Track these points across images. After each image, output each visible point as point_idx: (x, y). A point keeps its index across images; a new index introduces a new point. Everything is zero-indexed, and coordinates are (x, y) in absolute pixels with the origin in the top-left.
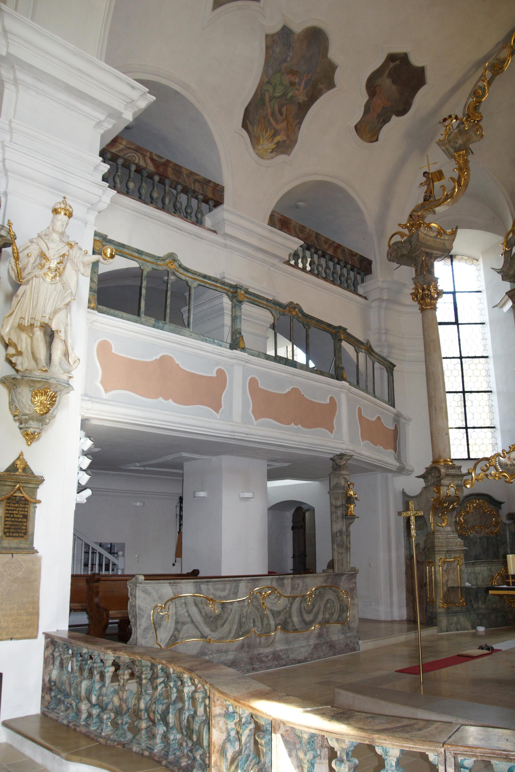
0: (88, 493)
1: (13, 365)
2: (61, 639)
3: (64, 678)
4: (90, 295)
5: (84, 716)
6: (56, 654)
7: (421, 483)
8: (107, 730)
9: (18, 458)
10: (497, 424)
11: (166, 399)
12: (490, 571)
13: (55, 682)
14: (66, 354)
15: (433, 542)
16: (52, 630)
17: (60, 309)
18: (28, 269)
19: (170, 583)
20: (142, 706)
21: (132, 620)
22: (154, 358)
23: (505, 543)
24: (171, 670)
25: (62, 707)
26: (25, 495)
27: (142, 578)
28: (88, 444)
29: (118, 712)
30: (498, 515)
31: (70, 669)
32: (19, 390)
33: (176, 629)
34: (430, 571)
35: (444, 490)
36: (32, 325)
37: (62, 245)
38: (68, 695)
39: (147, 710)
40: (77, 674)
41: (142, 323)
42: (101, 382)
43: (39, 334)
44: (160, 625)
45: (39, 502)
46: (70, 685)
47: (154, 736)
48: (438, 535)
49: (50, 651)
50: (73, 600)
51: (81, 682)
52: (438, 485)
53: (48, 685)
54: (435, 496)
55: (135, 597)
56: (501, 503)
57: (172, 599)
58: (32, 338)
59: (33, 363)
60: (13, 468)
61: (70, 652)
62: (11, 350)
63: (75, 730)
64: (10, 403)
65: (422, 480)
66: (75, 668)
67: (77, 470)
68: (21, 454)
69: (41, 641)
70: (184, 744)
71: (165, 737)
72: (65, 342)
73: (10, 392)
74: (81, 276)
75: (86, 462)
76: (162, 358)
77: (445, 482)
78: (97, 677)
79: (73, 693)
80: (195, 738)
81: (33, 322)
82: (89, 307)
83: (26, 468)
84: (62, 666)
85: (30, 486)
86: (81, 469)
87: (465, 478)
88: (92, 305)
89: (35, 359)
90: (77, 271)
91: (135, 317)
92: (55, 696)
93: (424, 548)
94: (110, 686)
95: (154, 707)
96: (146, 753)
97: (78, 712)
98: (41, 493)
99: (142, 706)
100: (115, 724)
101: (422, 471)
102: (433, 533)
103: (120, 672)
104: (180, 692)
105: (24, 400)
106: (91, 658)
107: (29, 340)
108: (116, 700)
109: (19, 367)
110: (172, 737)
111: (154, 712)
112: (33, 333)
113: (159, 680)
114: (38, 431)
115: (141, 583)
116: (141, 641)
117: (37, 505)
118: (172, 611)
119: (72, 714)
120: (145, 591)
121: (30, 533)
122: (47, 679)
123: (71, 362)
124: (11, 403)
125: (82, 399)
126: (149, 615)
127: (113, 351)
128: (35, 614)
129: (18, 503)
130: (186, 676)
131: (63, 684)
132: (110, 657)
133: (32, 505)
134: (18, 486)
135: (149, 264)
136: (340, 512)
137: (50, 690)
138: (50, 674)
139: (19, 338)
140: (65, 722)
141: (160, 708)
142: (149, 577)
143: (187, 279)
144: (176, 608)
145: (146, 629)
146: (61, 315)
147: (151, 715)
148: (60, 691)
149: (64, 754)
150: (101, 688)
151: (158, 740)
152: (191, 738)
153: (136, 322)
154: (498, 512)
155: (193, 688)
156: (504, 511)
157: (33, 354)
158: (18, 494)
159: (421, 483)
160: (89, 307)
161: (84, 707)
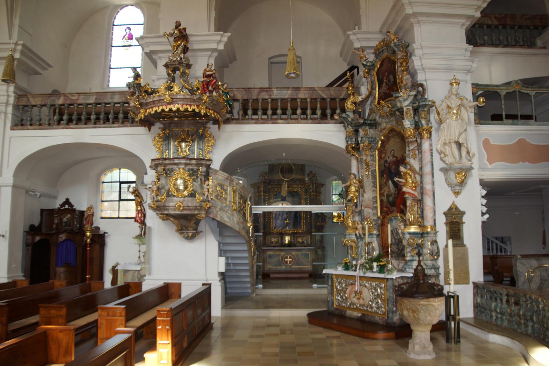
0: (487, 216)
1: (444, 162)
2: (481, 284)
3: (484, 302)
4: (475, 117)
5: (494, 318)
6: (479, 292)
8: (505, 323)
9: (453, 204)
11: (524, 162)
13: (479, 304)
14: (468, 153)
16: (476, 281)
17: (462, 133)
18: (444, 116)
19: (536, 259)
20: (521, 313)
21: (516, 278)
22: (514, 142)
24: (533, 297)
25: (484, 315)
26: (457, 220)
27: (519, 257)
28: (484, 192)
29: (511, 315)
31: (486, 298)
32: (449, 173)
33: (541, 283)
36: (450, 143)
37: (458, 100)
38: (486, 309)
39: (523, 315)
40: (490, 300)
41: (505, 124)
42: (487, 160)
43: (454, 146)
44: (531, 281)
45: (464, 223)
46: (487, 305)
47: (528, 326)
49: (475, 291)
50: (485, 268)
51: (492, 303)
53: (476, 305)
55: (517, 266)
57: (537, 268)
58: (451, 148)
59: (453, 159)
60: (451, 209)
61: (485, 290)
62: (442, 155)
63: (490, 323)
64: (445, 180)
66: (488, 297)
67: (480, 205)
68: (454, 202)
69: (471, 286)
70: (541, 329)
71: (533, 326)
72: (467, 148)
73: (445, 174)
74: (469, 113)
75: (484, 201)
76: (519, 140)
78: (499, 301)
79: (488, 308)
80: (545, 326)
81: (450, 141)
82: (475, 124)
83: (457, 208)
84: (482, 297)
85: (459, 216)
86: (482, 205)
88: (477, 122)
89: (454, 158)
90: (467, 110)
91: (500, 122)
92: (480, 310)
94: (505, 305)
95: (526, 313)
96: (524, 333)
97: (491, 316)
98: (465, 219)
99: (521, 313)
100: (510, 322)
103: (510, 298)
104: (538, 307)
105: (452, 178)
106: (496, 293)
107: (450, 149)
108: (509, 310)
109: (447, 162)
110: (536, 326)
111: (527, 316)
112: (451, 146)
113: (528, 302)
114: (460, 190)
115: (519, 259)
116: (521, 287)
117: (464, 224)
118: (538, 273)
119: (488, 317)
120: (522, 264)
121: (461, 237)
122: (475, 302)
123: (471, 156)
124: (446, 179)
125: (479, 171)
126: (525, 275)
127: (491, 143)
128: (467, 273)
129: (455, 224)
130: (540, 300)
131: (483, 304)
132: (504, 292)
133: (461, 225)
134: (454, 216)
135: (504, 91)
137: (477, 307)
138: (477, 300)
139: (445, 149)
140: (486, 320)
141: (529, 314)
142: (523, 256)
143: (528, 92)
144: (540, 272)
145: (524, 283)
146: (463, 135)
147: (526, 317)
148: (482, 308)
149: (487, 330)
150: (501, 306)
151: (530, 328)
152: (543, 326)
153: (501, 124)
155: (544, 305)
157: (452, 154)
158: (454, 220)
160: (475, 124)
161: (494, 314)
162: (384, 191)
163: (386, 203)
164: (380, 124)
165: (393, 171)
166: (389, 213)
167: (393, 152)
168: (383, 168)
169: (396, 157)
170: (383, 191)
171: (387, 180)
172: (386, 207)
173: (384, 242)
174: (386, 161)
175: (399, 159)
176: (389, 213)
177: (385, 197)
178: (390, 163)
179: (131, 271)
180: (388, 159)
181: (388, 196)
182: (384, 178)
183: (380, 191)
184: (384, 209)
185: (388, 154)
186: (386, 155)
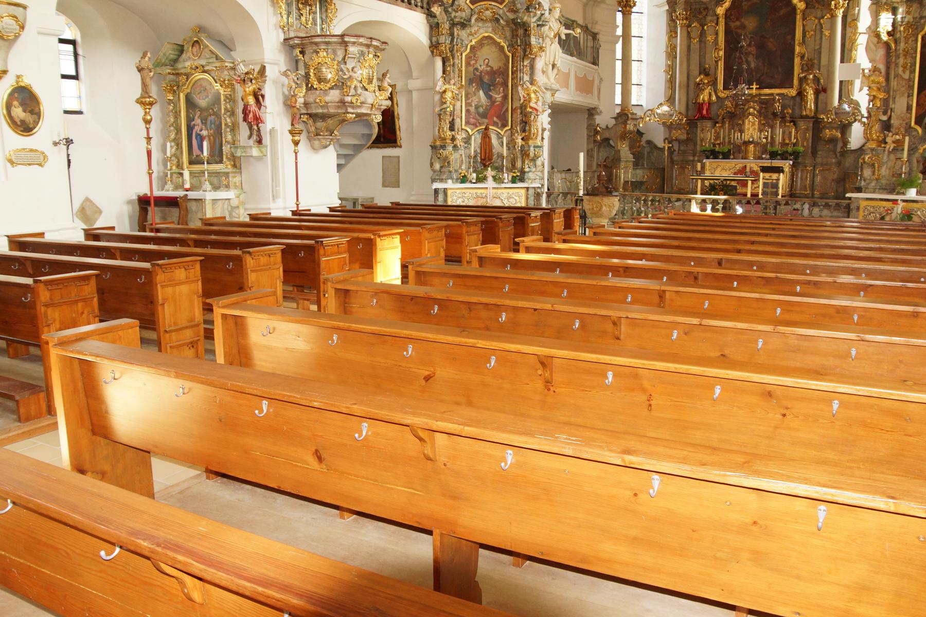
7: (613, 122)
10: (644, 82)
12: (643, 173)
15: (620, 156)
23: (643, 158)
30: (641, 141)
34: (617, 172)
35: (628, 127)
48: (621, 152)
52: (625, 123)
54: (622, 130)
56: (643, 134)
65: (614, 120)
77: (628, 122)
87: (638, 121)
93: (613, 159)
101: (615, 116)
102: (619, 151)
136: (592, 139)
154: (640, 139)
156: (644, 138)
159: (613, 122)
162: (472, 101)
163: (473, 114)
164: (471, 26)
165: (486, 80)
166: (478, 124)
167: (487, 60)
168: (472, 76)
169: (492, 68)
170: (470, 101)
171: (478, 90)
172: (474, 118)
173: (487, 155)
174: (477, 69)
175: (494, 70)
176: (478, 124)
177: (473, 108)
178: (481, 72)
179: (220, 202)
180: (479, 67)
181: (477, 107)
182: (474, 87)
183: (466, 101)
184: (471, 119)
185: (481, 62)
186: (476, 62)
